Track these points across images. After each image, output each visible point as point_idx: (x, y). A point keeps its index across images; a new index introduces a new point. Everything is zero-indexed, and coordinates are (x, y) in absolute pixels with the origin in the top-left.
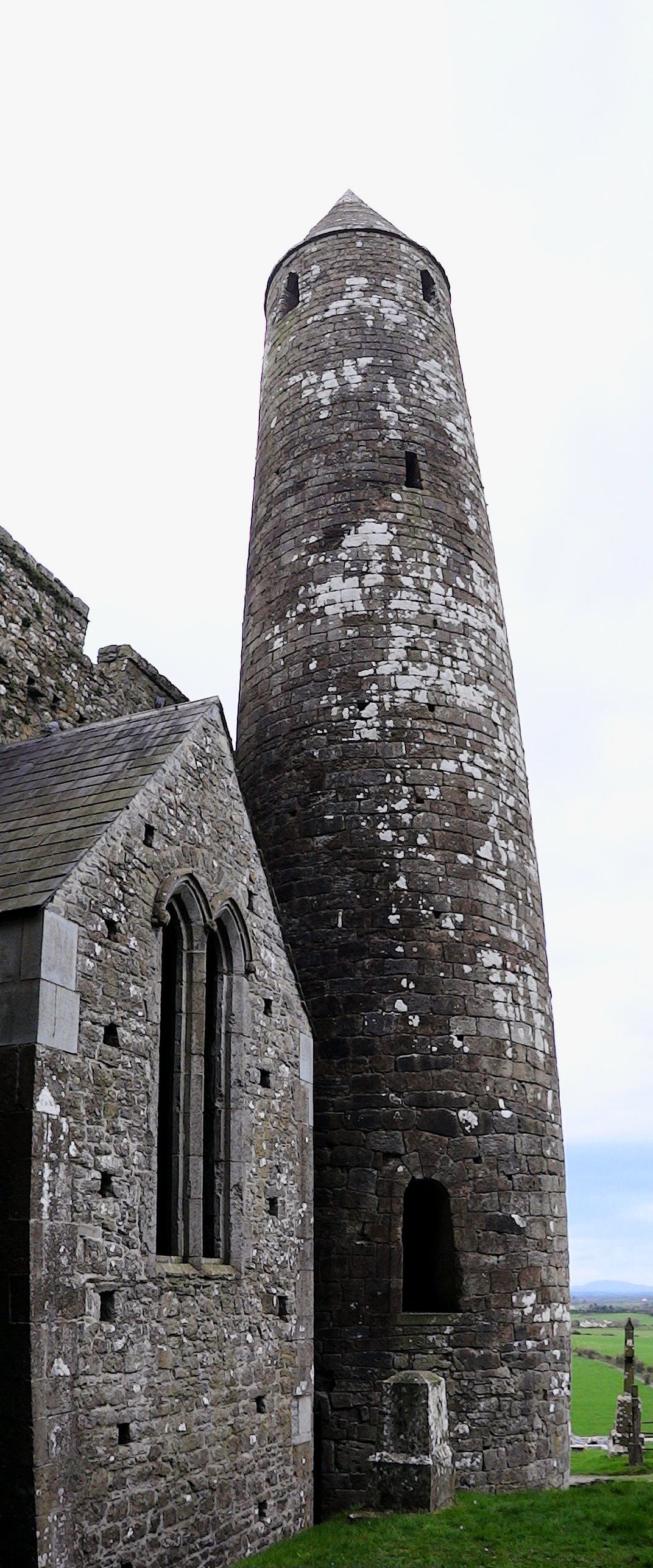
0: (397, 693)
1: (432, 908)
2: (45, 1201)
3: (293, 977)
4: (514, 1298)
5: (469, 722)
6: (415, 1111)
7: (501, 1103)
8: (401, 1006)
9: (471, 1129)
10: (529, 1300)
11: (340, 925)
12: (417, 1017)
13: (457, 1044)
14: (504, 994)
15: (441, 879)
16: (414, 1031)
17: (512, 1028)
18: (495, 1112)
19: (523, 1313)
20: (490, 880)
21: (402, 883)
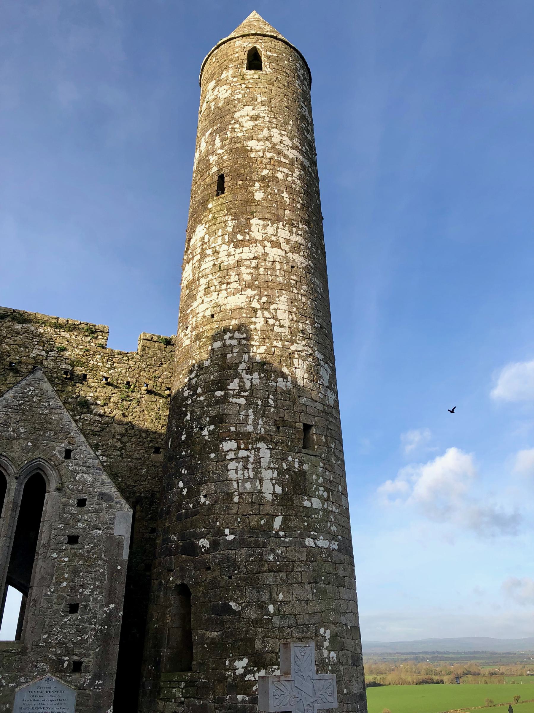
0: (198, 316)
1: (199, 426)
3: (112, 482)
4: (227, 663)
5: (232, 316)
6: (180, 543)
7: (227, 531)
8: (181, 484)
9: (205, 550)
10: (241, 664)
11: (169, 447)
12: (186, 489)
13: (203, 500)
14: (236, 464)
15: (205, 409)
16: (184, 497)
17: (240, 484)
18: (221, 538)
19: (234, 673)
20: (234, 400)
21: (188, 418)
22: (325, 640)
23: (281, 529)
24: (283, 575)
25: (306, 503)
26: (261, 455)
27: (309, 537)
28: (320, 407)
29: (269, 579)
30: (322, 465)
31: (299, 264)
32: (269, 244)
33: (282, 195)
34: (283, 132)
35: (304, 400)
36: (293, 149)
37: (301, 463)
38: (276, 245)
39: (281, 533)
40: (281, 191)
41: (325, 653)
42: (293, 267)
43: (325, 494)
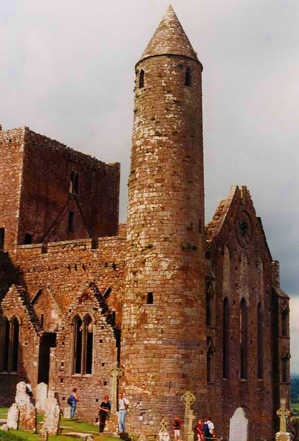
2: (52, 367)
22: (150, 378)
23: (136, 338)
24: (135, 354)
25: (146, 327)
26: (132, 309)
27: (146, 340)
28: (159, 282)
29: (133, 356)
30: (156, 309)
31: (152, 209)
32: (139, 204)
33: (147, 171)
34: (150, 128)
35: (148, 282)
36: (156, 136)
37: (145, 310)
38: (142, 203)
39: (136, 339)
40: (146, 169)
41: (149, 382)
42: (149, 212)
43: (156, 322)
